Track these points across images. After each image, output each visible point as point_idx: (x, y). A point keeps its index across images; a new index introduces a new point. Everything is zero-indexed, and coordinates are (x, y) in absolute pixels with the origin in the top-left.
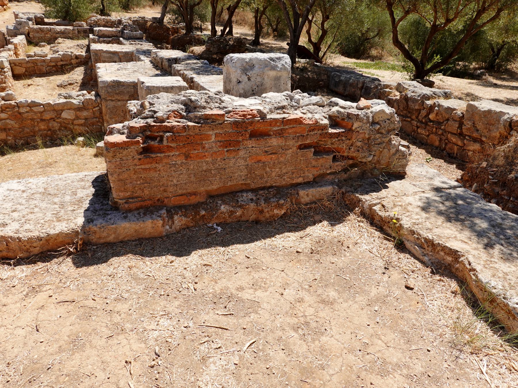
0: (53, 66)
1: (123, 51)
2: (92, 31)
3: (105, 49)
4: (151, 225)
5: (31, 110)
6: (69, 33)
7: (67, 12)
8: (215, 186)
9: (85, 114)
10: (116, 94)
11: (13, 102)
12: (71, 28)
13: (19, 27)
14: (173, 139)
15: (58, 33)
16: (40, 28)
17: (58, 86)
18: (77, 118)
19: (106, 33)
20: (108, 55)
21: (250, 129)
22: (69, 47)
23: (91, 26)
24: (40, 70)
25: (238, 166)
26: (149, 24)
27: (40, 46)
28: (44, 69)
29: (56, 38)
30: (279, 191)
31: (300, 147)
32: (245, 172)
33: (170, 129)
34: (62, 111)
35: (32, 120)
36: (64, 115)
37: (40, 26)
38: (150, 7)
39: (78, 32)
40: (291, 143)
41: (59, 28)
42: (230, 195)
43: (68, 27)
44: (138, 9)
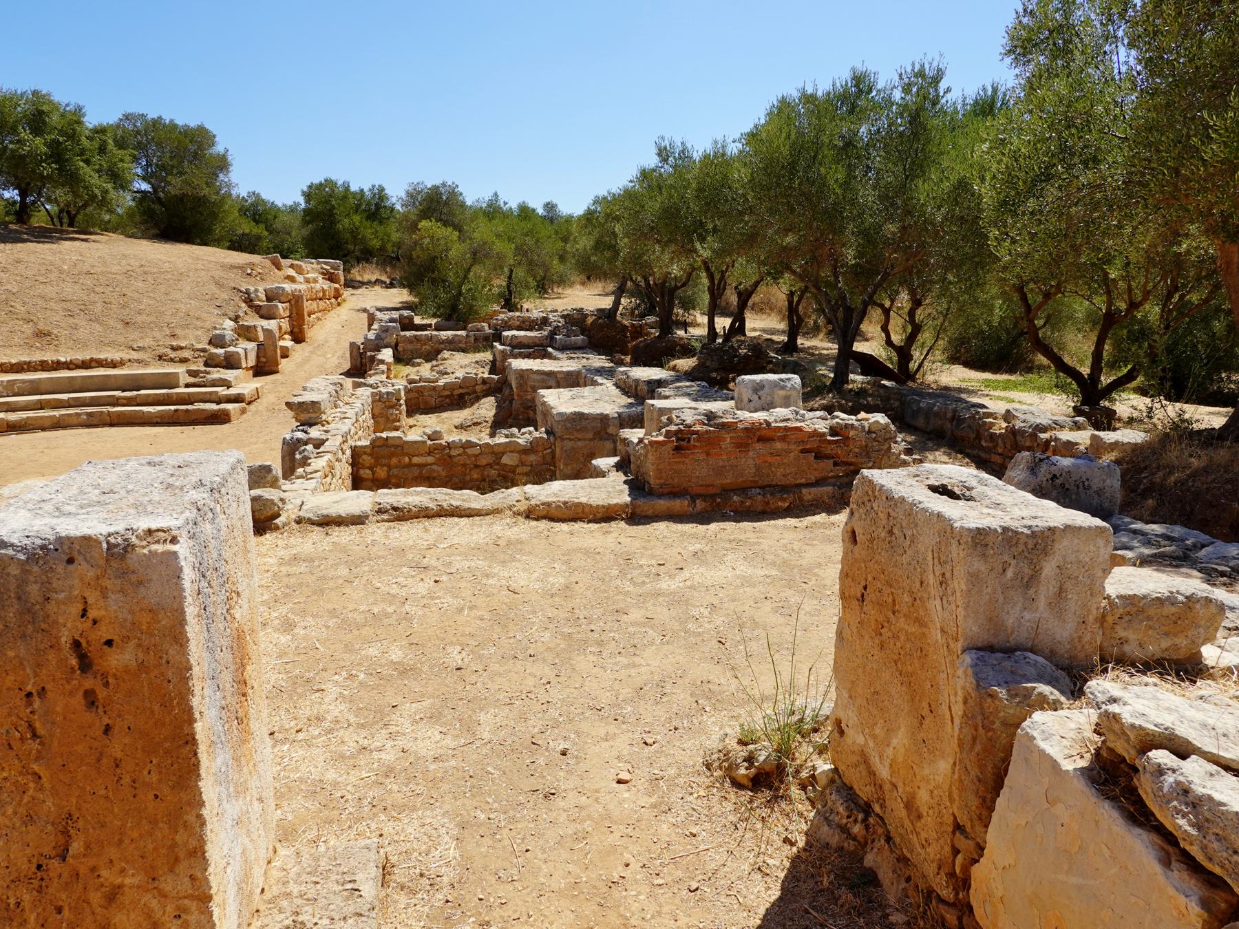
0: (447, 397)
1: (564, 369)
2: (498, 337)
3: (535, 368)
4: (679, 504)
5: (465, 453)
6: (460, 342)
7: (454, 308)
8: (728, 480)
9: (532, 458)
10: (577, 430)
11: (443, 442)
12: (463, 333)
13: (384, 335)
14: (698, 440)
15: (443, 342)
16: (415, 336)
17: (456, 427)
18: (523, 464)
19: (525, 341)
20: (539, 377)
21: (758, 434)
22: (462, 366)
23: (496, 330)
24: (426, 403)
25: (748, 464)
26: (590, 320)
27: (413, 365)
28: (432, 402)
29: (439, 352)
30: (785, 489)
31: (803, 451)
32: (753, 470)
33: (697, 432)
34: (503, 454)
35: (464, 465)
36: (506, 460)
37: (415, 333)
38: (583, 284)
39: (476, 339)
40: (793, 447)
41: (445, 334)
42: (743, 490)
43: (459, 333)
44: (560, 290)
